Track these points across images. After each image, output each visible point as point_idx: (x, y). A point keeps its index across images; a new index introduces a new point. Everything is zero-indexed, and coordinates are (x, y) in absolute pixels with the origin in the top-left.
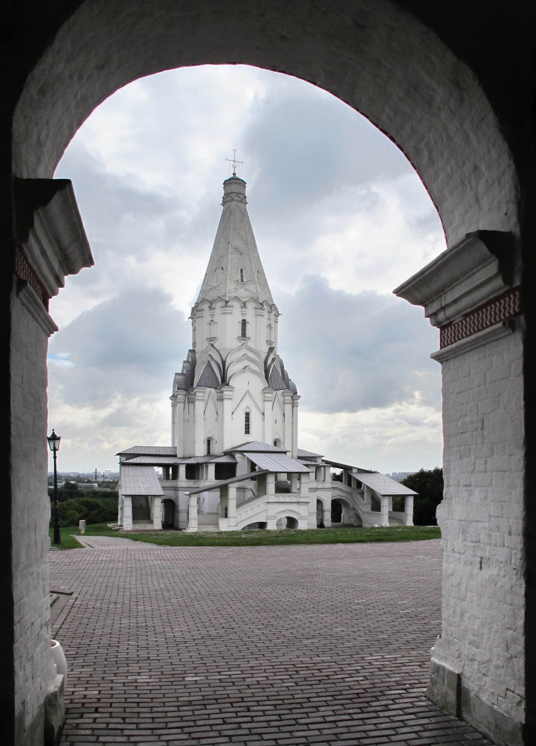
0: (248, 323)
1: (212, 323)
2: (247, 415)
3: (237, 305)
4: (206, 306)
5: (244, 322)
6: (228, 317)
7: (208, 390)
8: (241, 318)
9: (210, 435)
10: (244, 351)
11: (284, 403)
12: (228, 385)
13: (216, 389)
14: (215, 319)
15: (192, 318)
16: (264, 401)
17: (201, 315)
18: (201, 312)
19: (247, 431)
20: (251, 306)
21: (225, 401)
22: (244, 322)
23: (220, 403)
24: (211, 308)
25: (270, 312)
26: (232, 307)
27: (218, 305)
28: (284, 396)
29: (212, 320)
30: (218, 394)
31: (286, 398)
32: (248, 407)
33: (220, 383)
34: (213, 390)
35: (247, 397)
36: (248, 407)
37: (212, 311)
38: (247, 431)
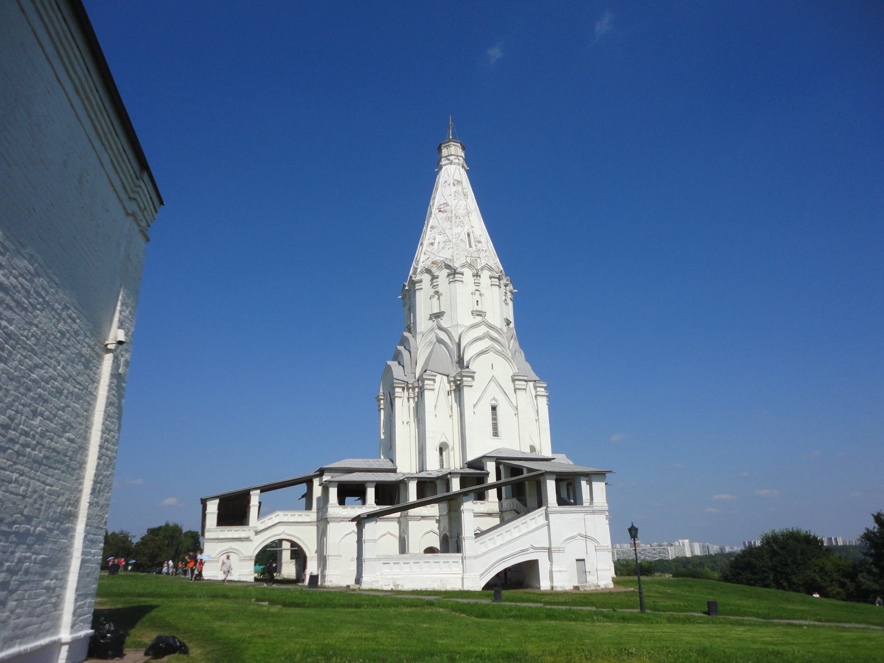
2: (494, 408)
3: (468, 273)
6: (458, 284)
7: (438, 378)
9: (444, 440)
11: (536, 396)
12: (468, 367)
13: (448, 376)
14: (440, 289)
16: (515, 390)
19: (496, 434)
20: (485, 274)
24: (434, 278)
25: (506, 286)
26: (462, 274)
28: (535, 388)
29: (437, 292)
31: (538, 389)
32: (494, 399)
34: (445, 378)
36: (494, 399)
38: (496, 434)
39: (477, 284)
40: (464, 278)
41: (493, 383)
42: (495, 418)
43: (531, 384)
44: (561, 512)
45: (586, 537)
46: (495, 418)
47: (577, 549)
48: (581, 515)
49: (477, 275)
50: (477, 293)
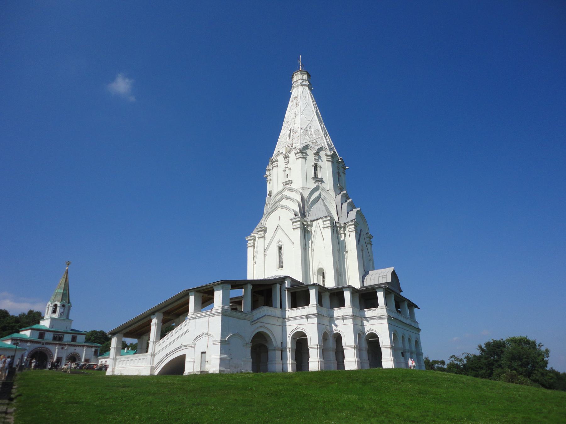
2: (280, 248)
10: (287, 193)
19: (281, 266)
32: (279, 241)
38: (281, 266)
39: (287, 163)
40: (279, 163)
41: (279, 231)
42: (280, 255)
43: (320, 221)
44: (195, 318)
45: (208, 334)
46: (280, 255)
47: (201, 345)
48: (206, 319)
49: (286, 157)
50: (287, 169)
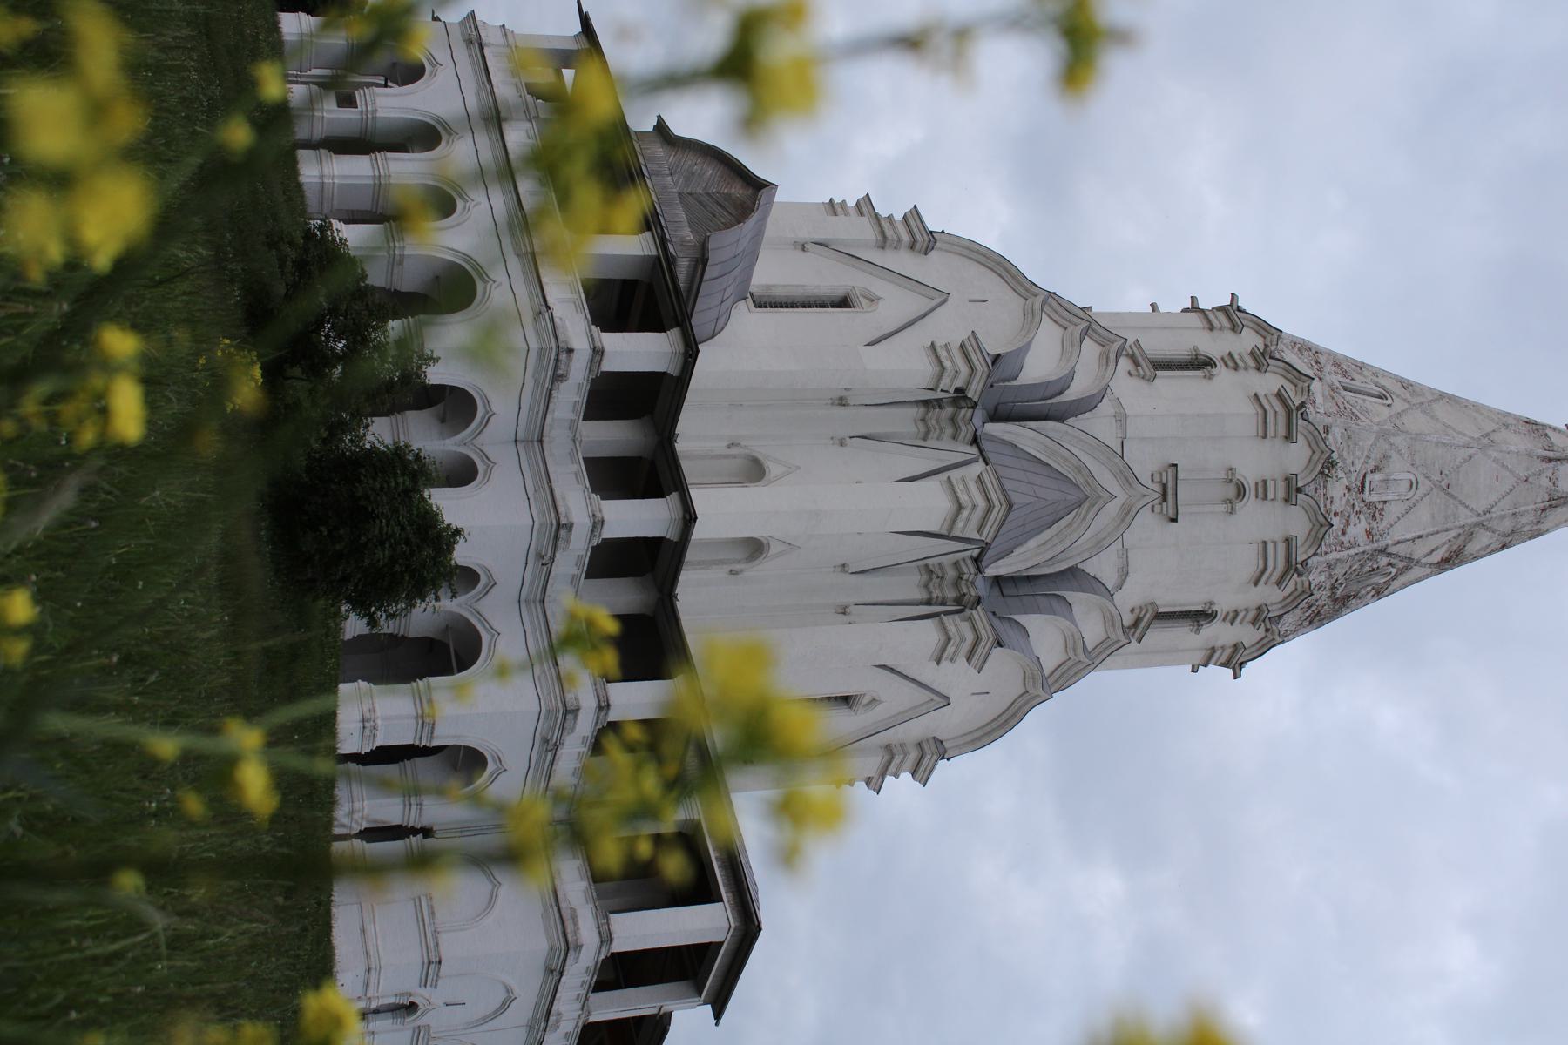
0: (1198, 631)
1: (1231, 491)
2: (846, 700)
4: (1296, 457)
5: (1200, 617)
8: (1223, 605)
9: (774, 549)
15: (1233, 314)
16: (888, 748)
17: (1271, 433)
18: (1282, 431)
21: (927, 633)
22: (1200, 617)
23: (909, 587)
27: (1296, 522)
29: (1241, 491)
30: (951, 574)
33: (991, 571)
35: (925, 695)
37: (1281, 494)
